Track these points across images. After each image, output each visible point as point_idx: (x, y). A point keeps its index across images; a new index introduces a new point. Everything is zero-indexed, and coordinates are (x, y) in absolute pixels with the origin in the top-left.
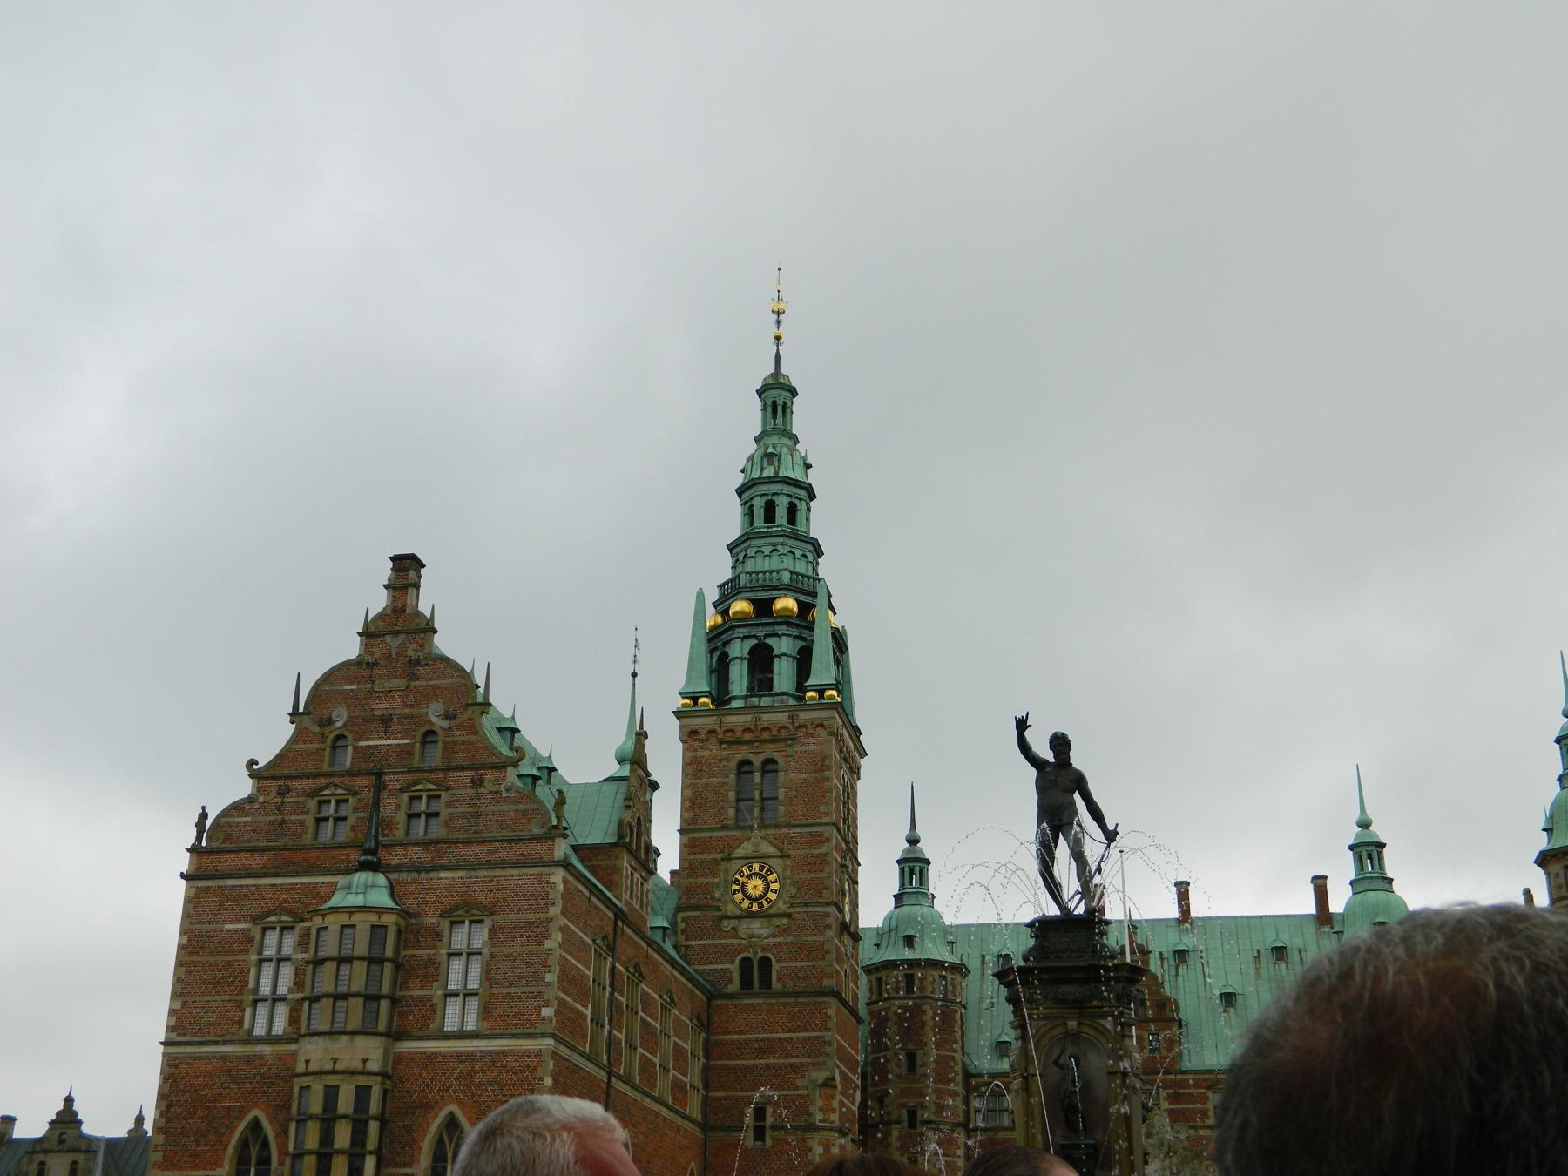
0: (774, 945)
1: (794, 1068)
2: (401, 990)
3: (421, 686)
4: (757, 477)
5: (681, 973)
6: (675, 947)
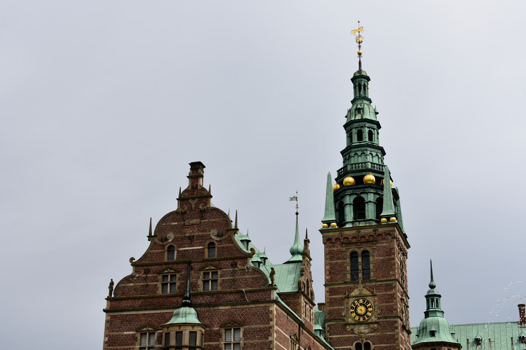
0: (371, 337)
3: (206, 222)
4: (353, 119)
6: (325, 339)
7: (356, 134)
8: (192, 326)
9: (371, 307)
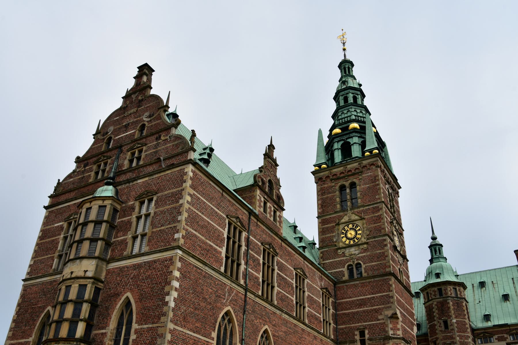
0: (362, 257)
1: (376, 311)
2: (114, 239)
5: (311, 265)
7: (343, 100)
8: (102, 200)
9: (360, 230)
